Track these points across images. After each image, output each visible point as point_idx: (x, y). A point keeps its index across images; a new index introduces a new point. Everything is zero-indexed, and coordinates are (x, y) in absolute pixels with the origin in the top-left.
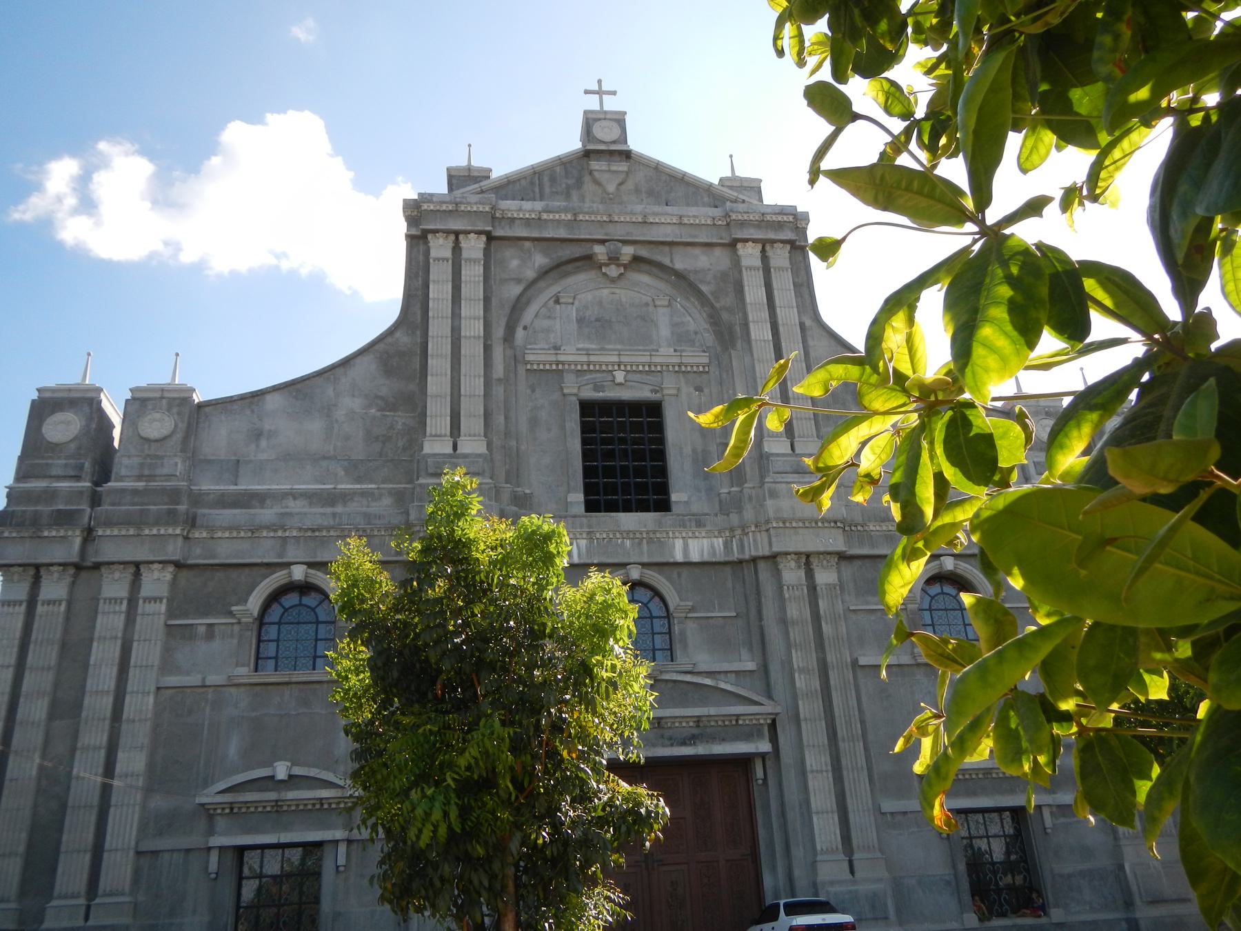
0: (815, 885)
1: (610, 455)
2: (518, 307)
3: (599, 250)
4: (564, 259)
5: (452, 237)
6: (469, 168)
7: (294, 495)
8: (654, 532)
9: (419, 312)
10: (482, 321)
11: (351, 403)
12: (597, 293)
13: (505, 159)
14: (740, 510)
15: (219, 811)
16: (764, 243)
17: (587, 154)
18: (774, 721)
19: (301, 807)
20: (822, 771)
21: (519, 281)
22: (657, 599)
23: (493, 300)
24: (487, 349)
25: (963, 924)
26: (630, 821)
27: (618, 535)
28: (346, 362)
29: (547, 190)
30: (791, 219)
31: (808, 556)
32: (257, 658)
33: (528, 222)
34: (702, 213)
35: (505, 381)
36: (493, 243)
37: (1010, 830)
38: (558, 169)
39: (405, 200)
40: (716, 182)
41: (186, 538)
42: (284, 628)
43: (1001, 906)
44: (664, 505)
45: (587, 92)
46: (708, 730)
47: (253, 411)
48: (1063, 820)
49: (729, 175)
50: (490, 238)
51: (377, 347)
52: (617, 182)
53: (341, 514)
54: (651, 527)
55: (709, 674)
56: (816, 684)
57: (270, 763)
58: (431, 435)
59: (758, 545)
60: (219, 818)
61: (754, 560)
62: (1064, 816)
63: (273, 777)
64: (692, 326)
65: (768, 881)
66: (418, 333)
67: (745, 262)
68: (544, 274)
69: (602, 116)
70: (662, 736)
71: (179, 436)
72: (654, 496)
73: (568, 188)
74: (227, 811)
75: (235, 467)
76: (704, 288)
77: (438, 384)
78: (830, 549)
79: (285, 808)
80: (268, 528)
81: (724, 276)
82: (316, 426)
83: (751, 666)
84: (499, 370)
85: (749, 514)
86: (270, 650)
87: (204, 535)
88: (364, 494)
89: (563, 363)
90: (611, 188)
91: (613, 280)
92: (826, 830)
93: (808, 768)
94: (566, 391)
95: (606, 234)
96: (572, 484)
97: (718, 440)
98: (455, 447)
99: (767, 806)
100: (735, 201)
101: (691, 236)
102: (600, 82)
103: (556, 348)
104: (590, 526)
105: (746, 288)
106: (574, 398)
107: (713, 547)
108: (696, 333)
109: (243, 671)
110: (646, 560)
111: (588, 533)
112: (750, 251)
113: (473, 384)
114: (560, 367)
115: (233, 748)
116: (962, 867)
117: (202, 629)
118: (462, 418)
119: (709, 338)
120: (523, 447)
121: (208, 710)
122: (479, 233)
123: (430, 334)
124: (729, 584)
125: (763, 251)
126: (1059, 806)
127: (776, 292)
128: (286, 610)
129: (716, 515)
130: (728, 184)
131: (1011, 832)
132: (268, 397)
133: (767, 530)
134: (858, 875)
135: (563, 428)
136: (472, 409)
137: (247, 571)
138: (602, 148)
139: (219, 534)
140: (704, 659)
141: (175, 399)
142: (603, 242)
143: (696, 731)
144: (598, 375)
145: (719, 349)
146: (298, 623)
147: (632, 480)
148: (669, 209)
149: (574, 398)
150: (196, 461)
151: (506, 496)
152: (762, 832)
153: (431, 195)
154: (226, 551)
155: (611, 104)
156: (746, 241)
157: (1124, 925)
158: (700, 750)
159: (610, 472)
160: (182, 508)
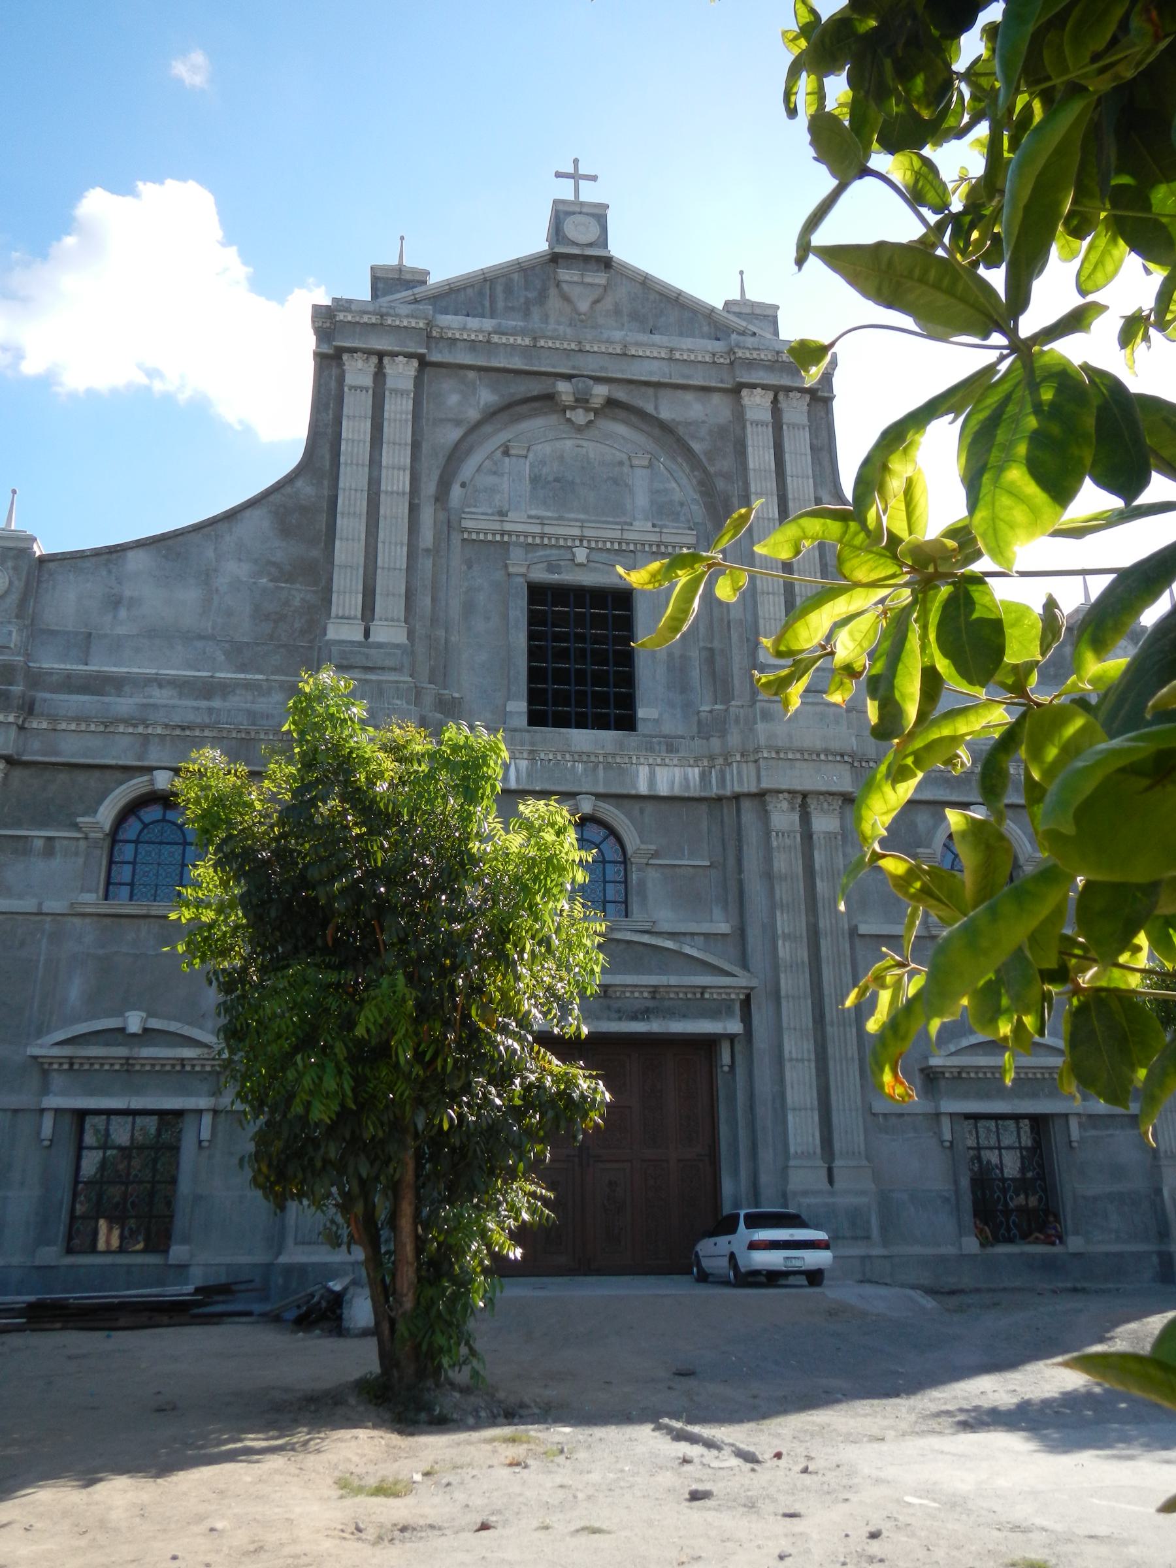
0: (784, 1195)
1: (563, 655)
2: (455, 456)
3: (563, 387)
4: (518, 397)
5: (374, 360)
6: (400, 269)
7: (160, 682)
8: (614, 756)
9: (328, 456)
10: (408, 472)
11: (235, 569)
12: (558, 444)
13: (447, 261)
14: (723, 733)
15: (55, 1066)
16: (777, 390)
17: (554, 259)
18: (748, 996)
19: (158, 1068)
20: (802, 1060)
21: (458, 423)
22: (612, 839)
23: (425, 448)
24: (413, 509)
25: (960, 1248)
26: (564, 1107)
27: (568, 757)
28: (231, 516)
29: (500, 305)
31: (805, 795)
32: (108, 883)
33: (473, 345)
34: (700, 347)
35: (435, 551)
36: (428, 369)
37: (1027, 1141)
38: (515, 276)
39: (315, 307)
40: (719, 305)
41: (21, 728)
42: (143, 848)
43: (1009, 1230)
44: (627, 723)
45: (558, 175)
46: (667, 1004)
47: (110, 572)
48: (1093, 1133)
49: (739, 298)
50: (424, 363)
51: (271, 498)
52: (590, 300)
53: (219, 710)
54: (610, 749)
55: (672, 935)
56: (803, 954)
57: (120, 1014)
58: (337, 617)
59: (742, 780)
60: (55, 1075)
61: (737, 797)
62: (1095, 1127)
63: (122, 1030)
64: (678, 496)
65: (727, 1187)
66: (326, 483)
67: (750, 415)
68: (491, 415)
69: (578, 209)
70: (609, 1008)
71: (14, 598)
72: (614, 708)
73: (527, 302)
74: (66, 1067)
75: (85, 642)
76: (697, 447)
77: (348, 550)
78: (834, 789)
79: (138, 1068)
80: (126, 722)
81: (721, 432)
82: (190, 595)
83: (724, 928)
84: (427, 537)
85: (734, 739)
86: (125, 873)
87: (45, 725)
88: (248, 686)
89: (510, 533)
90: (584, 306)
91: (579, 429)
92: (802, 1131)
93: (787, 1055)
94: (511, 570)
95: (574, 368)
96: (514, 689)
97: (702, 644)
98: (367, 634)
99: (732, 1098)
100: (743, 333)
101: (683, 376)
102: (576, 162)
103: (502, 513)
104: (532, 744)
105: (750, 450)
106: (521, 580)
107: (686, 779)
108: (682, 504)
109: (90, 897)
110: (601, 789)
111: (531, 752)
113: (393, 553)
114: (506, 538)
115: (75, 991)
116: (965, 1182)
117: (39, 844)
118: (377, 597)
119: (698, 511)
120: (453, 639)
121: (45, 940)
122: (409, 356)
123: (341, 485)
124: (704, 826)
125: (775, 401)
126: (1090, 1116)
127: (787, 457)
128: (146, 826)
129: (693, 738)
130: (736, 309)
131: (1029, 1144)
132: (130, 554)
133: (756, 761)
134: (837, 1185)
135: (505, 617)
136: (391, 584)
137: (97, 774)
138: (576, 254)
139: (63, 726)
140: (666, 917)
141: (10, 549)
142: (569, 377)
143: (651, 1004)
144: (554, 552)
145: (709, 526)
146: (161, 843)
147: (588, 689)
148: (656, 338)
149: (521, 580)
150: (35, 631)
151: (428, 700)
152: (724, 1130)
153: (350, 301)
154: (73, 747)
155: (589, 194)
156: (754, 386)
157: (1155, 1259)
158: (655, 1026)
159: (561, 676)
160: (17, 689)
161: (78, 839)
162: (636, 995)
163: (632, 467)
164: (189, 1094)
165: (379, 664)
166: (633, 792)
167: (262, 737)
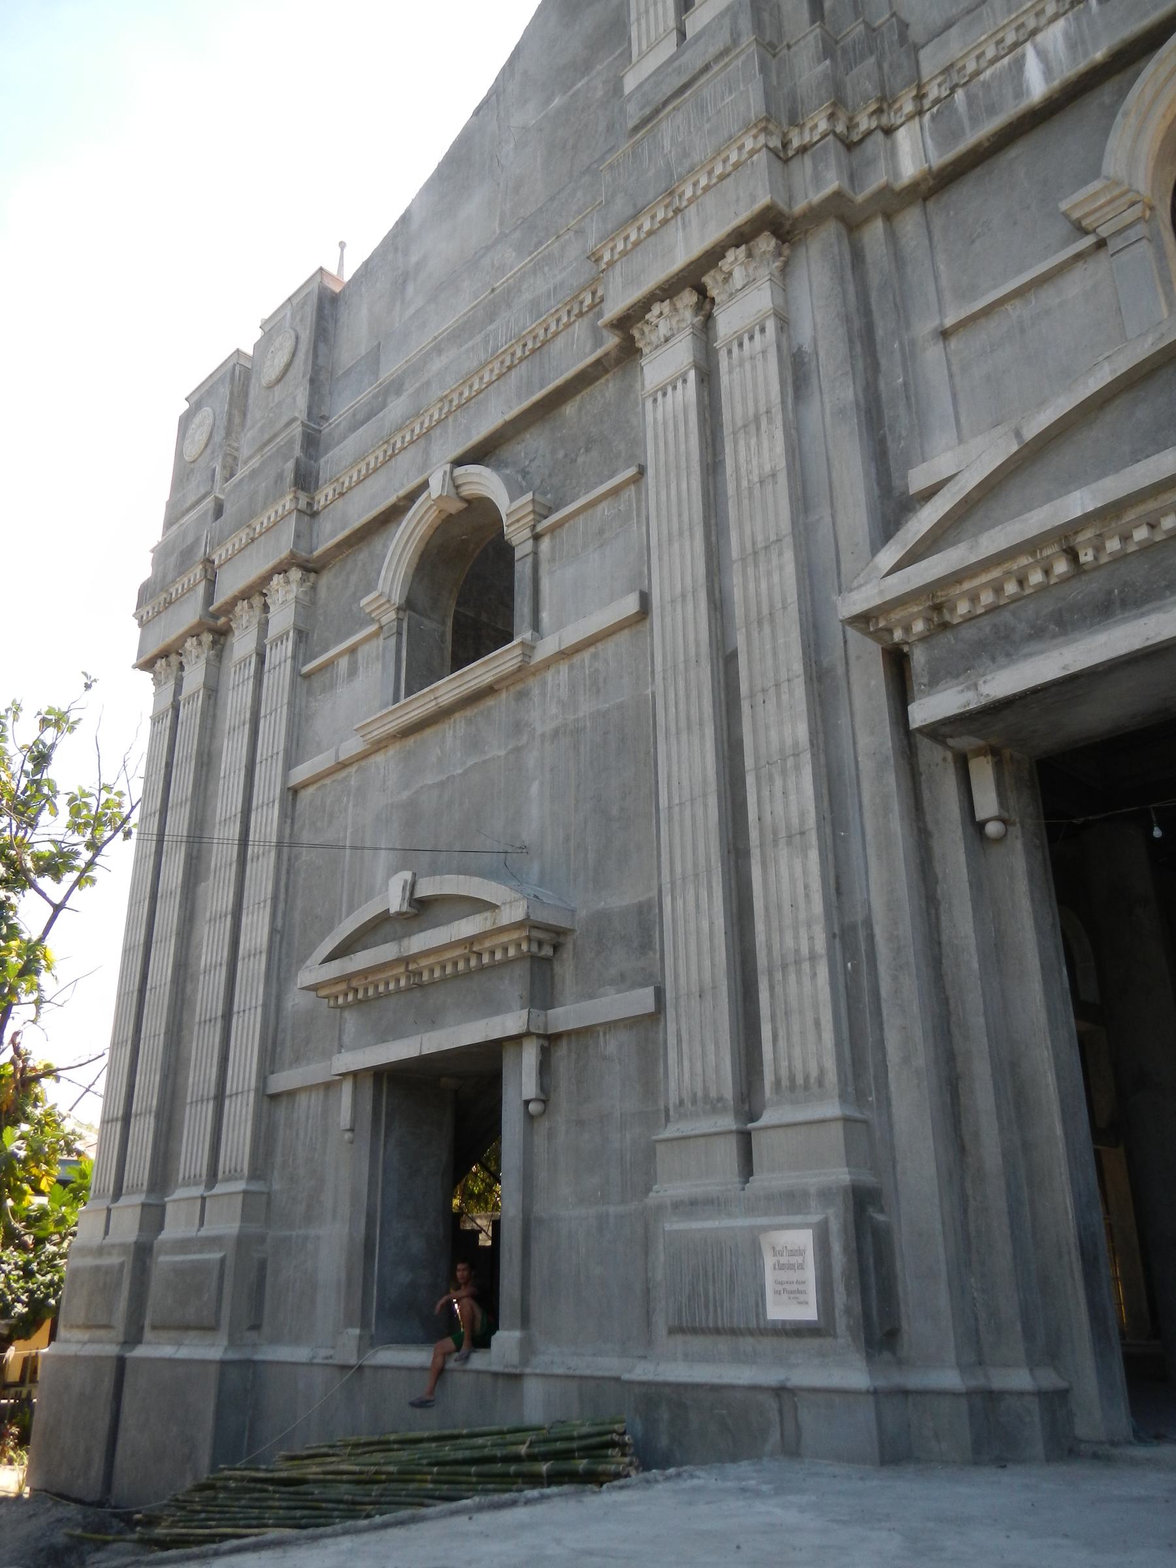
75: (374, 358)
161: (376, 634)
164: (492, 1006)
165: (699, 65)
167: (553, 328)
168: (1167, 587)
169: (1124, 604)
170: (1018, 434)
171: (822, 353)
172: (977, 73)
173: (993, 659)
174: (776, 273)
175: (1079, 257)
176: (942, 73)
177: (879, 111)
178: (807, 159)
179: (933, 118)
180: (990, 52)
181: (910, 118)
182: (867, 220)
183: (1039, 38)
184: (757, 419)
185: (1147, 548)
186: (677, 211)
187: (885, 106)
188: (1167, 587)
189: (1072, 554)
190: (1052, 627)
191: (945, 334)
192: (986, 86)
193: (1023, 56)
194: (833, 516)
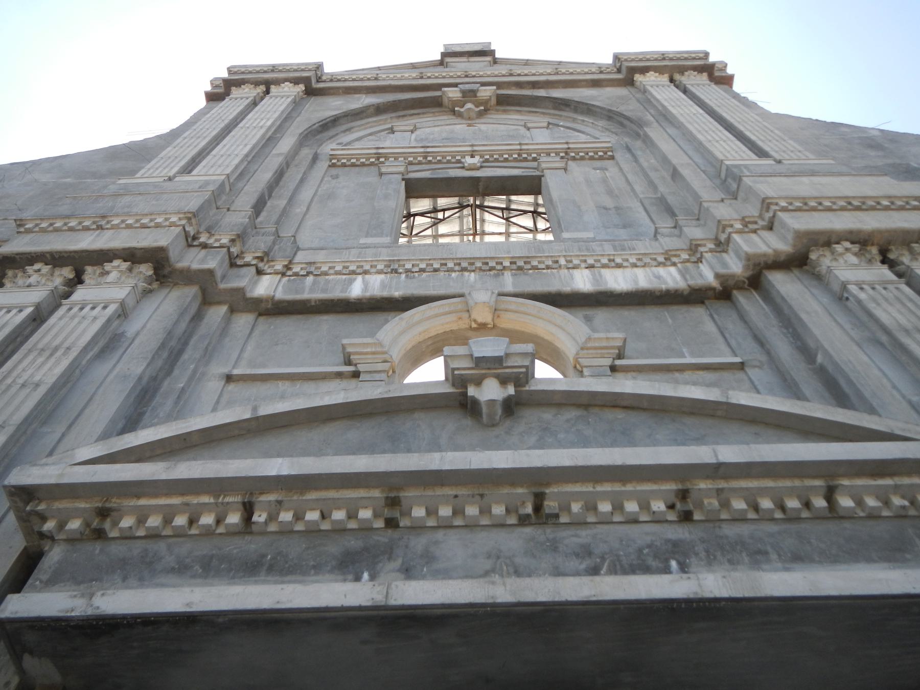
30: (701, 55)
46: (730, 531)
91: (469, 119)
94: (383, 170)
112: (653, 78)
125: (672, 80)
162: (631, 507)
163: (528, 129)
166: (567, 289)
168: (314, 567)
169: (271, 569)
170: (255, 409)
171: (137, 342)
172: (326, 274)
173: (125, 579)
174: (140, 289)
175: (339, 375)
176: (307, 263)
177: (261, 259)
178: (204, 252)
179: (289, 281)
180: (339, 268)
181: (276, 273)
182: (219, 303)
183: (367, 276)
184: (56, 349)
185: (313, 532)
186: (100, 227)
187: (265, 259)
188: (314, 567)
189: (248, 509)
190: (197, 567)
191: (229, 378)
192: (328, 282)
193: (355, 279)
194: (63, 435)
